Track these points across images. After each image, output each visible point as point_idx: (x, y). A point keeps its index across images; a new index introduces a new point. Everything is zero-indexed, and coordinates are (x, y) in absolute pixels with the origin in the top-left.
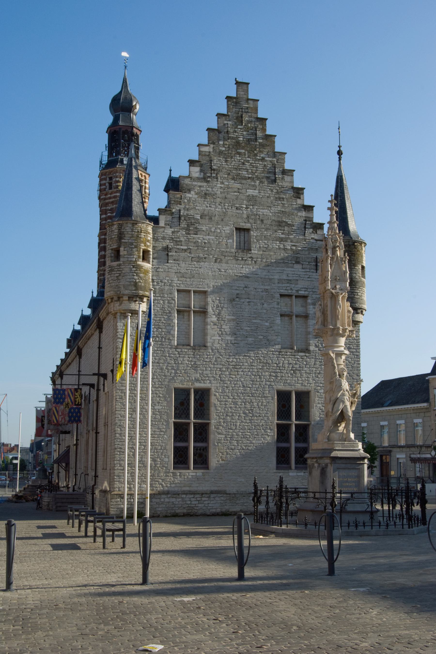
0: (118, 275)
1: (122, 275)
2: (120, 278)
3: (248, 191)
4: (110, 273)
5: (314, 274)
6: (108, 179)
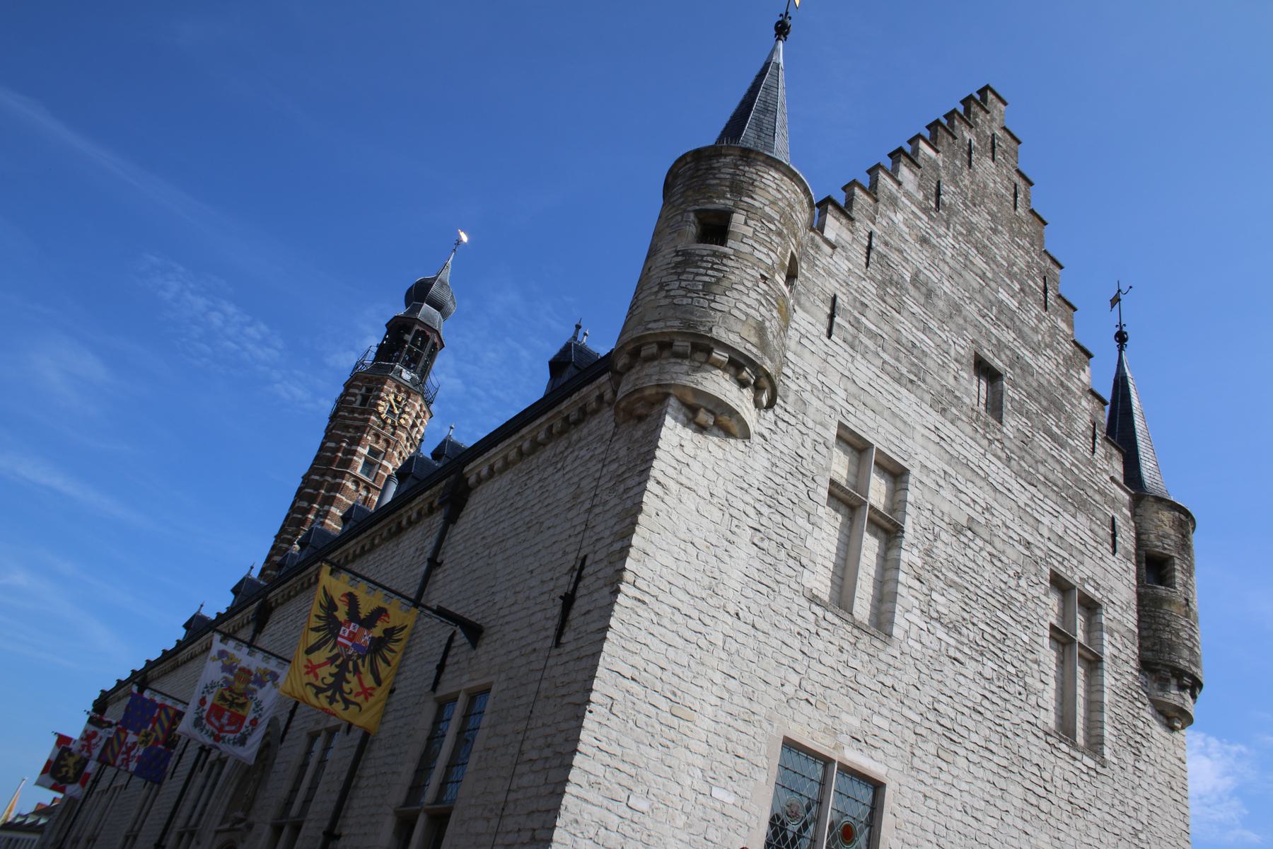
0: (713, 280)
1: (726, 283)
2: (716, 289)
3: (1000, 290)
4: (679, 270)
5: (1110, 556)
6: (364, 390)
